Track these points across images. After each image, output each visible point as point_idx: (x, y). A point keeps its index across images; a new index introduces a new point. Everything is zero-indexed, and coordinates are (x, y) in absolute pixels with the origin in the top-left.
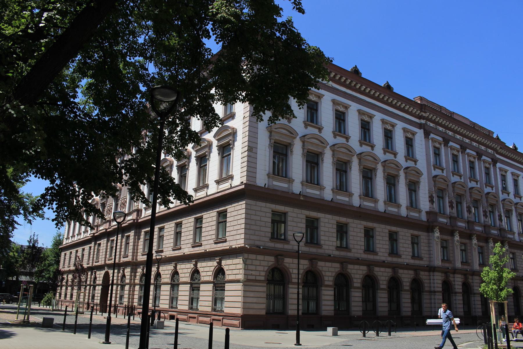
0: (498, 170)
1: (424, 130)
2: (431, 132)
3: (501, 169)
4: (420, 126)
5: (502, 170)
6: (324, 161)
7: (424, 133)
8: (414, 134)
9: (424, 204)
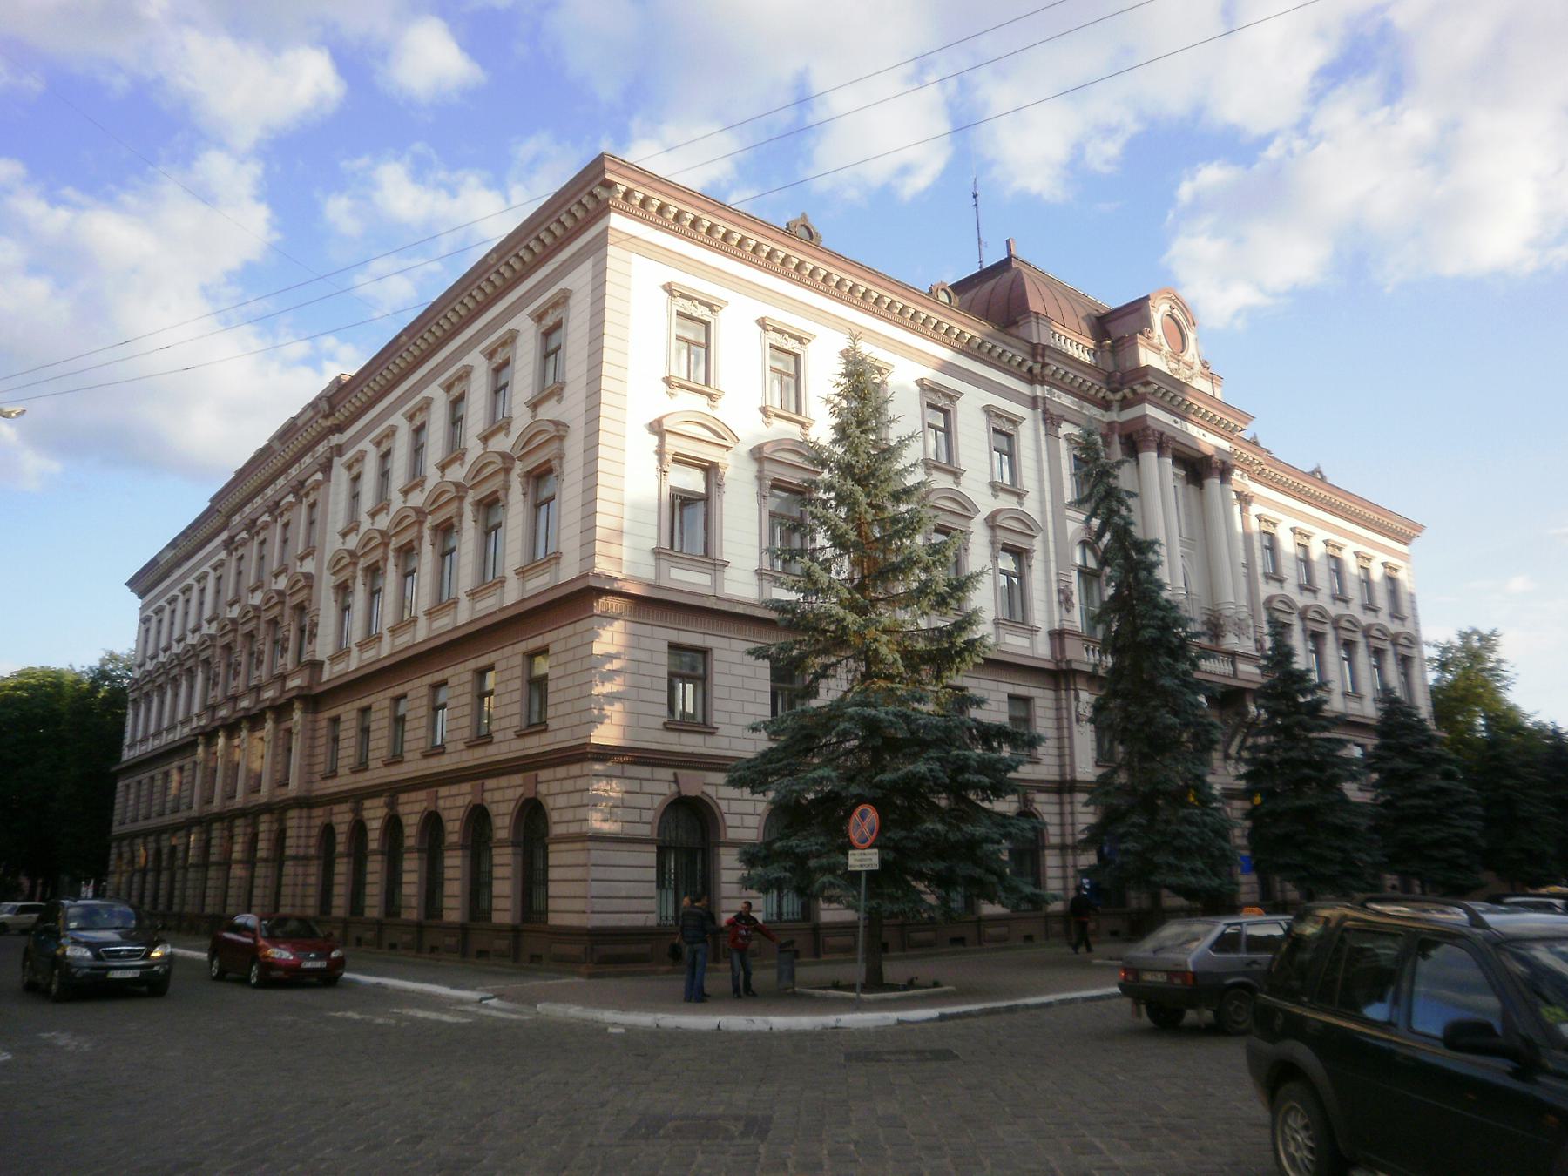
1: (1045, 412)
2: (1062, 418)
4: (1034, 402)
7: (1045, 420)
8: (1015, 421)
9: (1043, 612)
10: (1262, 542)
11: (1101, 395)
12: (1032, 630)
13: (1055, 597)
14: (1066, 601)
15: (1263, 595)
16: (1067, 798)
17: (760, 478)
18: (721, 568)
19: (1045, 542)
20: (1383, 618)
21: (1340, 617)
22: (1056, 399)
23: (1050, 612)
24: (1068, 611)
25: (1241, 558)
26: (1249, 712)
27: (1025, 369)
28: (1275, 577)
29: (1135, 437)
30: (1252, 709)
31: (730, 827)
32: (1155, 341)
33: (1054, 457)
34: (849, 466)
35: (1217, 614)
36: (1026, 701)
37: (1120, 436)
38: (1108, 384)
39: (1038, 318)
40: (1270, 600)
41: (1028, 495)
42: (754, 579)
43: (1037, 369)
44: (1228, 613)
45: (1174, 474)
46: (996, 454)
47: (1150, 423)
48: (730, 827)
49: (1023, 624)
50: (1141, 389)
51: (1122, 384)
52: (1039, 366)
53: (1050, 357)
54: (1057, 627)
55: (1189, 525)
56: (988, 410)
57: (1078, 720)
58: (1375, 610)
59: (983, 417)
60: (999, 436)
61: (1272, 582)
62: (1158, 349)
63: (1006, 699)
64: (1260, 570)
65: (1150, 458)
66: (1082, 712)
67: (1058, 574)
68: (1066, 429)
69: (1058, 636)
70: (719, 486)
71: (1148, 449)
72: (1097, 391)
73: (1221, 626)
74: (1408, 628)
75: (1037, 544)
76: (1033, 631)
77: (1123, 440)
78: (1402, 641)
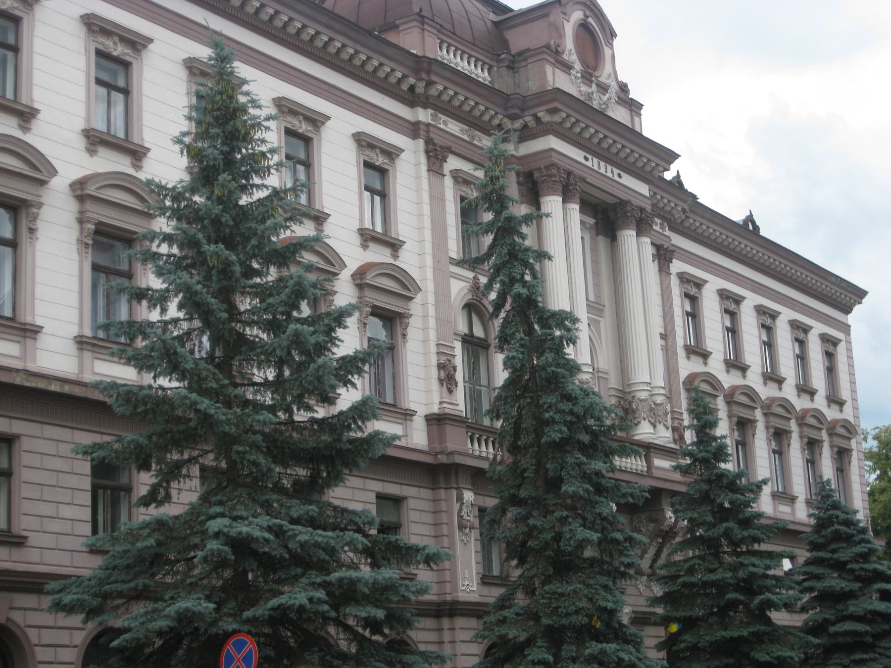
0: (674, 282)
1: (429, 142)
3: (684, 278)
4: (413, 130)
5: (688, 281)
6: (39, 234)
7: (427, 152)
8: (391, 153)
10: (683, 306)
11: (496, 122)
12: (406, 415)
13: (434, 372)
14: (447, 380)
15: (683, 374)
16: (446, 622)
17: (81, 221)
18: (32, 335)
19: (425, 304)
20: (820, 402)
21: (772, 400)
22: (442, 126)
23: (428, 391)
24: (450, 391)
25: (657, 327)
26: (665, 518)
27: (405, 87)
28: (698, 351)
29: (536, 175)
30: (669, 514)
31: (40, 663)
32: (565, 57)
33: (437, 199)
34: (216, 222)
35: (629, 397)
36: (397, 501)
37: (518, 174)
38: (506, 108)
39: (423, 23)
40: (691, 378)
41: (405, 247)
42: (72, 348)
43: (420, 88)
44: (643, 395)
45: (582, 223)
46: (367, 194)
47: (555, 159)
48: (40, 663)
49: (394, 406)
50: (546, 118)
51: (523, 110)
52: (423, 84)
53: (438, 75)
54: (435, 409)
55: (597, 285)
56: (362, 141)
57: (461, 527)
58: (812, 393)
59: (352, 146)
60: (372, 172)
61: (693, 357)
62: (567, 67)
63: (374, 500)
64: (680, 342)
65: (552, 203)
66: (465, 517)
67: (438, 345)
68: (453, 163)
69: (436, 421)
70: (32, 231)
71: (553, 192)
72: (492, 117)
73: (634, 411)
74: (848, 413)
75: (415, 307)
76: (407, 415)
77: (521, 179)
78: (841, 431)
